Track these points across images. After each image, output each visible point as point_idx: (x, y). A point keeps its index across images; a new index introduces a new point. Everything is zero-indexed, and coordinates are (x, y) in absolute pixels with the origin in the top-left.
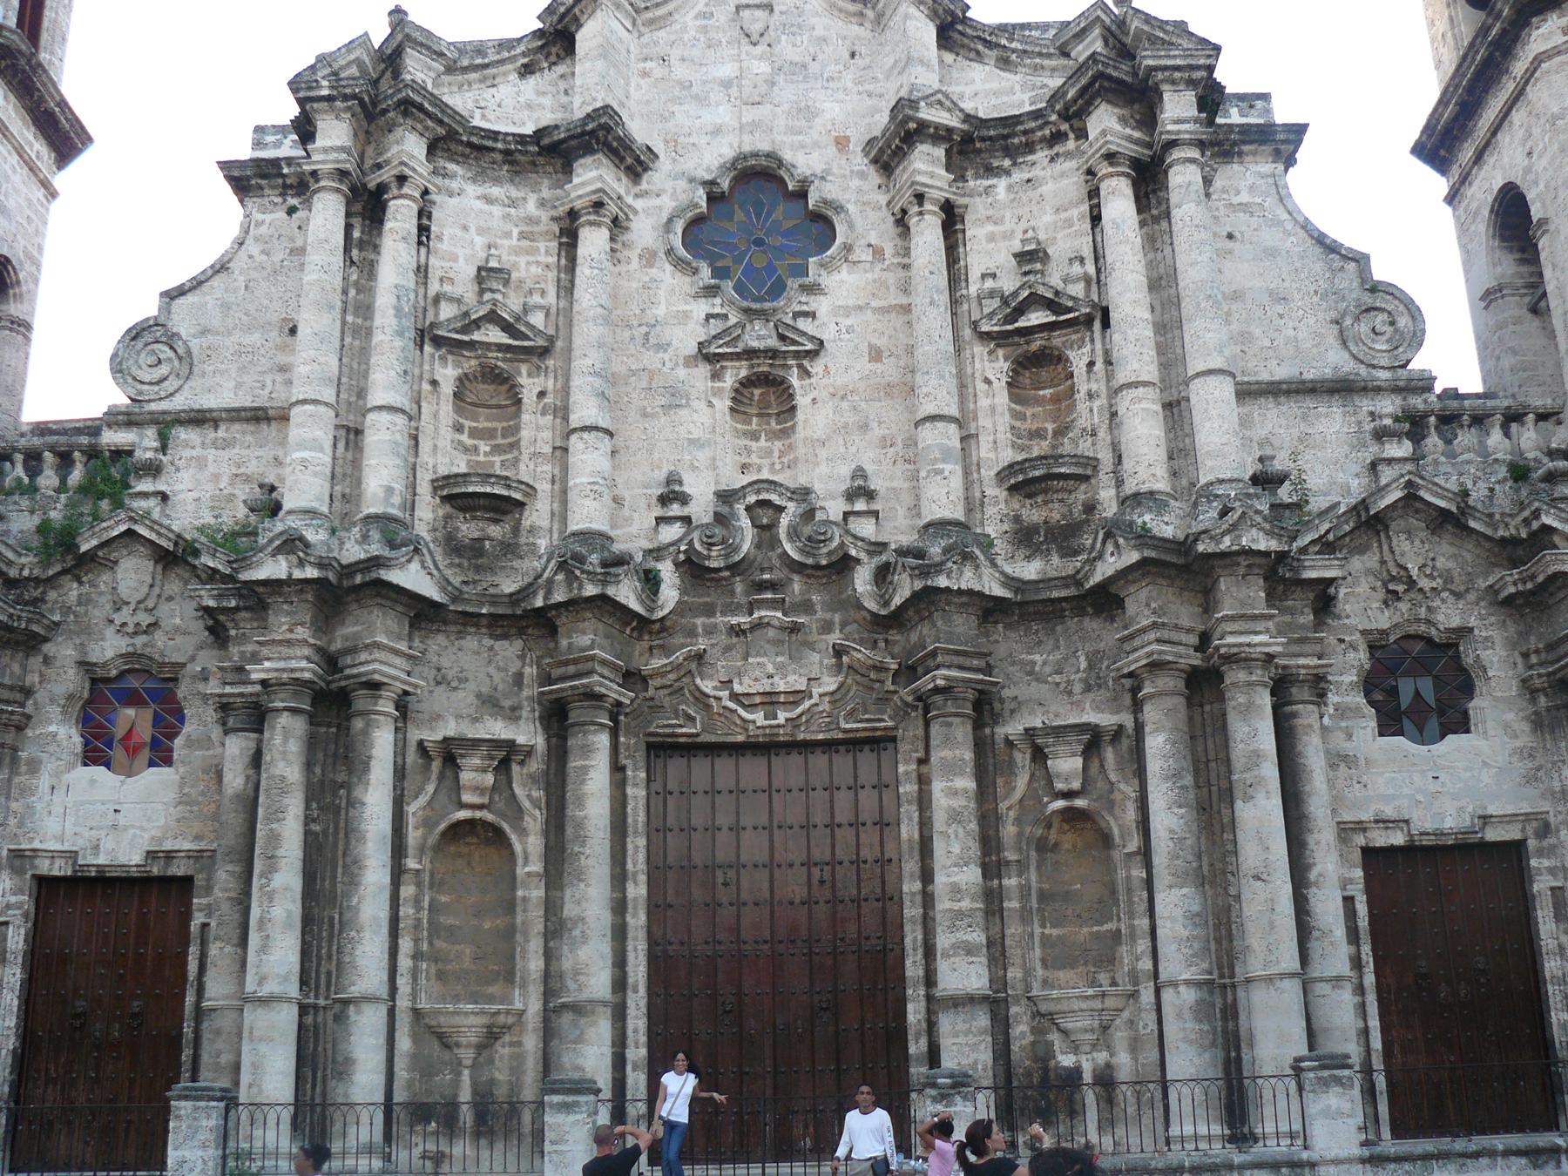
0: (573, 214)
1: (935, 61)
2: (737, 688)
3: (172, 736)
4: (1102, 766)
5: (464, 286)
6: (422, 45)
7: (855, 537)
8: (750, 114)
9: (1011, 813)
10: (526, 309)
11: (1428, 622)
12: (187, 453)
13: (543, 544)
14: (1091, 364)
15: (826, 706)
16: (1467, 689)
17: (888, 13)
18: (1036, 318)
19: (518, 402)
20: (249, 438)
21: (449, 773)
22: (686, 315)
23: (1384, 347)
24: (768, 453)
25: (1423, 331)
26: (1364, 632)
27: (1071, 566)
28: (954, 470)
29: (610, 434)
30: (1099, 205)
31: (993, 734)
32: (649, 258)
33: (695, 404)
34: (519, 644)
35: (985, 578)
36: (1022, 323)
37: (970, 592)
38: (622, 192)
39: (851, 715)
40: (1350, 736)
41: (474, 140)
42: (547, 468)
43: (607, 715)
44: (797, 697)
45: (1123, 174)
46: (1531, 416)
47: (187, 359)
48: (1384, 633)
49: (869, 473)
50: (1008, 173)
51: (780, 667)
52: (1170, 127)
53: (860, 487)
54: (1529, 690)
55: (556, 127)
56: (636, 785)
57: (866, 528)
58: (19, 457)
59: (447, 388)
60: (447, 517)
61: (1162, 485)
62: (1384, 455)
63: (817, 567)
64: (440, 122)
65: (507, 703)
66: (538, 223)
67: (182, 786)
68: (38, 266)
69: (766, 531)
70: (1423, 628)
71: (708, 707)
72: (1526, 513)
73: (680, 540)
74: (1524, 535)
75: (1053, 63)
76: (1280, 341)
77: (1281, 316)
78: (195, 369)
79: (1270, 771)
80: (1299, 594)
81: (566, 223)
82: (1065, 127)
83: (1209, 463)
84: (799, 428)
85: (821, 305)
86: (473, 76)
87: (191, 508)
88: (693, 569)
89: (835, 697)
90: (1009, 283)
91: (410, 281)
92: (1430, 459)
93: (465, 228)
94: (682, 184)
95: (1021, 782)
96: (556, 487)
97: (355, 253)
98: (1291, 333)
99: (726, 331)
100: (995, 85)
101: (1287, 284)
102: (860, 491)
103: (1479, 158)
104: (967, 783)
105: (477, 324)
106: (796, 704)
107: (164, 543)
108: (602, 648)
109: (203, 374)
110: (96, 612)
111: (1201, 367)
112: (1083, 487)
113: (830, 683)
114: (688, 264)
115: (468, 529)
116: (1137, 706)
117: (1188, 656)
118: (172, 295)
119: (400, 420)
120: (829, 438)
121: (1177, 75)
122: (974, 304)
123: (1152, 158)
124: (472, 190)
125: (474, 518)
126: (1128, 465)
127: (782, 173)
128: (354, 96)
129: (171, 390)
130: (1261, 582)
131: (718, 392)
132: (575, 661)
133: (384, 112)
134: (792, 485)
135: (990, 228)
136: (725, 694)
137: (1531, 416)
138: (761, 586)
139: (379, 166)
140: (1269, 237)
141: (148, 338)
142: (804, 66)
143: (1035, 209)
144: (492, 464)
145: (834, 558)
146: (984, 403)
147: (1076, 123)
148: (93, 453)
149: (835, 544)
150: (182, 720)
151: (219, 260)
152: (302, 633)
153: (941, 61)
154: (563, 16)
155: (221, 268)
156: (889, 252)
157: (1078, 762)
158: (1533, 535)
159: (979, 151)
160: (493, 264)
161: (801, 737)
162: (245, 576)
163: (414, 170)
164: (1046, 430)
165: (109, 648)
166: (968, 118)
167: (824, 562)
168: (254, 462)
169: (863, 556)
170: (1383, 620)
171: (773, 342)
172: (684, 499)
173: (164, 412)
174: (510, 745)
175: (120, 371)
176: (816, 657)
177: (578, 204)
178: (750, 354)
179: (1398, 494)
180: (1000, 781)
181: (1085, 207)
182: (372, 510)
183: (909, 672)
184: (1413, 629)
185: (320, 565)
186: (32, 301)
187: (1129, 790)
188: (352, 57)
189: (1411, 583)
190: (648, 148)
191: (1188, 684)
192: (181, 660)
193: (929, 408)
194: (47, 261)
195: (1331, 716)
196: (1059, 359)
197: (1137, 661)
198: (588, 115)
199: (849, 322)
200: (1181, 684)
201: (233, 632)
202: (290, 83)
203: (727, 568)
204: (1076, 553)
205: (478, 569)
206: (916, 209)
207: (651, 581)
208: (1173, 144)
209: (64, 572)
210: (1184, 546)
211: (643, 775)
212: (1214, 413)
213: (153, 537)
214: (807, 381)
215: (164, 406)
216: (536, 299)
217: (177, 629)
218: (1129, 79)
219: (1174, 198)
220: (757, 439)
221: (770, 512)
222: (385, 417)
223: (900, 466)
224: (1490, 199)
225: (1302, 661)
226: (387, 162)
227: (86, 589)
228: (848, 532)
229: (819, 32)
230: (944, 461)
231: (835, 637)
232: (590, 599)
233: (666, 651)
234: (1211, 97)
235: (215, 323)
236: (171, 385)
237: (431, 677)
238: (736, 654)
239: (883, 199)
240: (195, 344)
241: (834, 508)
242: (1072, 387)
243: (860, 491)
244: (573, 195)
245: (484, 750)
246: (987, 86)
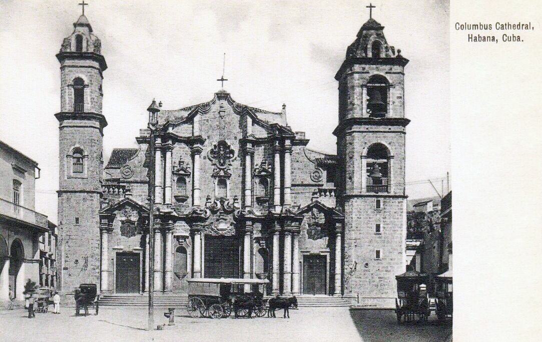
5: (177, 165)
10: (187, 168)
18: (263, 173)
32: (205, 158)
52: (286, 146)
57: (236, 205)
59: (176, 181)
136: (216, 228)
138: (221, 213)
165: (124, 219)
178: (220, 176)
207: (206, 213)
215: (129, 180)
216: (188, 166)
234: (292, 139)
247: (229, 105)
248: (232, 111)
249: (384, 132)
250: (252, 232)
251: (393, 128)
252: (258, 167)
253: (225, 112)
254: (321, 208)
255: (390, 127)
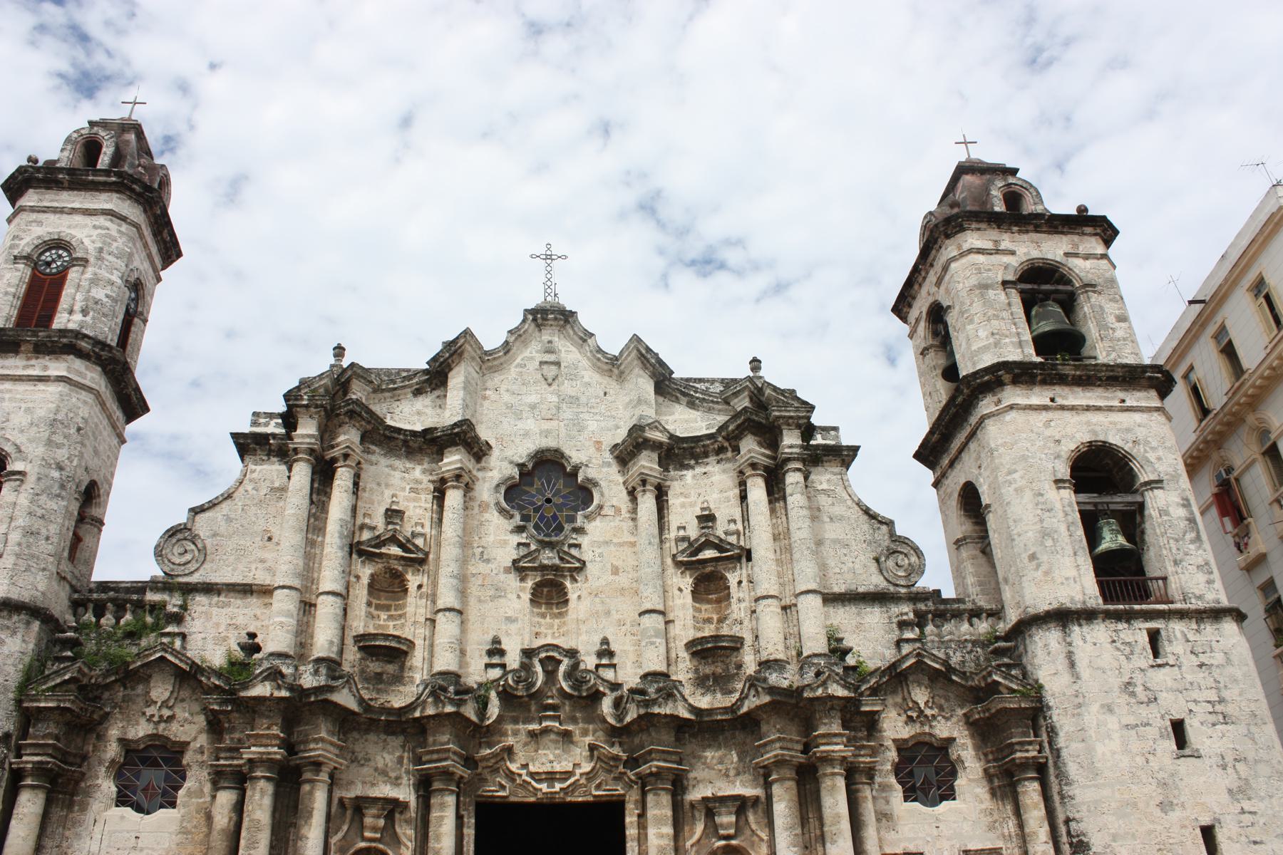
0: (443, 481)
1: (653, 402)
2: (532, 768)
3: (177, 788)
4: (747, 820)
5: (379, 521)
6: (362, 377)
7: (603, 679)
8: (547, 425)
9: (694, 849)
11: (930, 734)
12: (199, 609)
13: (418, 677)
14: (740, 582)
15: (583, 781)
16: (954, 774)
17: (627, 372)
18: (709, 554)
19: (406, 591)
20: (239, 602)
21: (357, 818)
22: (505, 542)
23: (903, 574)
24: (551, 626)
25: (924, 565)
26: (894, 741)
27: (728, 701)
28: (660, 641)
29: (460, 612)
30: (745, 490)
31: (683, 800)
32: (484, 507)
33: (509, 596)
34: (401, 738)
35: (680, 708)
36: (701, 556)
37: (672, 716)
38: (471, 467)
39: (598, 787)
40: (888, 802)
41: (387, 433)
42: (422, 631)
43: (454, 784)
44: (569, 774)
45: (762, 476)
46: (984, 615)
47: (203, 551)
48: (905, 741)
49: (611, 641)
50: (693, 468)
51: (557, 757)
52: (787, 450)
53: (606, 650)
54: (988, 776)
55: (436, 429)
56: (469, 827)
57: (609, 675)
58: (91, 606)
59: (365, 580)
60: (362, 659)
61: (781, 656)
62: (904, 637)
63: (580, 697)
64: (369, 422)
65: (393, 775)
66: (421, 483)
67: (182, 822)
68: (110, 485)
69: (550, 675)
70: (927, 739)
71: (513, 780)
72: (984, 673)
73: (500, 678)
74: (983, 685)
75: (720, 407)
76: (845, 568)
77: (845, 555)
78: (208, 557)
79: (845, 825)
80: (858, 718)
81: (438, 485)
82: (726, 444)
83: (809, 644)
84: (570, 613)
85: (584, 541)
86: (387, 394)
87: (200, 643)
88: (507, 696)
89: (590, 776)
90: (693, 532)
91: (348, 517)
92: (929, 638)
93: (379, 484)
94: (505, 464)
95: (699, 828)
96: (427, 642)
97: (314, 497)
98: (851, 565)
99: (529, 554)
100: (686, 417)
101: (849, 537)
102: (606, 652)
103: (952, 464)
104: (668, 830)
105: (384, 543)
106: (566, 779)
107: (183, 666)
108: (453, 743)
109: (213, 561)
110: (134, 707)
111: (804, 588)
112: (735, 654)
113: (587, 767)
114: (508, 512)
115: (374, 667)
116: (767, 786)
117: (798, 757)
118: (196, 511)
119: (338, 601)
120: (587, 619)
121: (790, 421)
122: (673, 544)
123: (776, 465)
124: (384, 461)
125: (377, 660)
126: (763, 643)
127: (563, 461)
128: (322, 406)
129: (192, 569)
130: (839, 714)
131: (523, 589)
132: (438, 751)
133: (338, 415)
134: (566, 646)
135: (682, 499)
136: (524, 772)
137: (984, 615)
139: (333, 447)
140: (838, 510)
141: (180, 536)
142: (578, 399)
143: (708, 490)
144: (388, 627)
145: (591, 692)
146: (679, 602)
147: (734, 443)
148: (139, 606)
149: (592, 682)
150: (184, 778)
151: (227, 491)
152: (275, 731)
153: (656, 401)
154: (442, 363)
155: (228, 496)
156: (624, 511)
157: (733, 818)
158: (988, 685)
159: (677, 455)
160: (394, 507)
161: (569, 799)
162: (243, 694)
163: (353, 451)
164: (712, 618)
165: (140, 730)
166: (672, 437)
167: (585, 694)
168: (241, 617)
169: (607, 691)
170: (905, 732)
171: (557, 561)
172: (502, 653)
173: (187, 584)
174: (395, 802)
175: (161, 556)
176: (578, 751)
177: (447, 475)
178: (543, 568)
179: (912, 661)
180: (687, 828)
181: (737, 491)
182: (321, 655)
183: (633, 763)
184: (922, 739)
185: (291, 688)
186: (105, 507)
187: (764, 836)
188: (322, 383)
189: (921, 712)
190: (487, 443)
191: (797, 773)
192: (188, 740)
193: (649, 606)
194: (116, 482)
195: (877, 790)
196: (724, 578)
197: (768, 759)
198: (455, 424)
199: (600, 551)
200: (794, 775)
201: (226, 725)
202: (285, 396)
203: (527, 696)
204: (731, 692)
205: (379, 691)
206: (640, 489)
207: (483, 704)
208: (788, 460)
209: (116, 681)
210: (794, 693)
211: (473, 821)
212: (811, 615)
213: (177, 662)
214: (576, 585)
216: (419, 529)
217: (186, 720)
218: (764, 421)
219: (789, 490)
220: (543, 616)
221: (553, 663)
222: (331, 598)
223: (629, 637)
224: (958, 488)
225: (862, 759)
226: (338, 445)
227: (129, 692)
228: (599, 677)
229: (586, 379)
230: (656, 636)
231: (589, 739)
232: (449, 714)
233: (490, 745)
234: (808, 431)
235: (223, 530)
236: (192, 567)
237: (348, 757)
238: (532, 746)
239: (621, 480)
240: (208, 542)
241: (589, 661)
242: (729, 594)
243: (606, 652)
244: (444, 469)
245: (380, 805)
246: (682, 417)
247: (573, 349)
248: (585, 363)
249: (1110, 409)
250: (678, 785)
251: (1134, 398)
252: (682, 533)
253: (558, 364)
254: (940, 678)
255: (1121, 395)
